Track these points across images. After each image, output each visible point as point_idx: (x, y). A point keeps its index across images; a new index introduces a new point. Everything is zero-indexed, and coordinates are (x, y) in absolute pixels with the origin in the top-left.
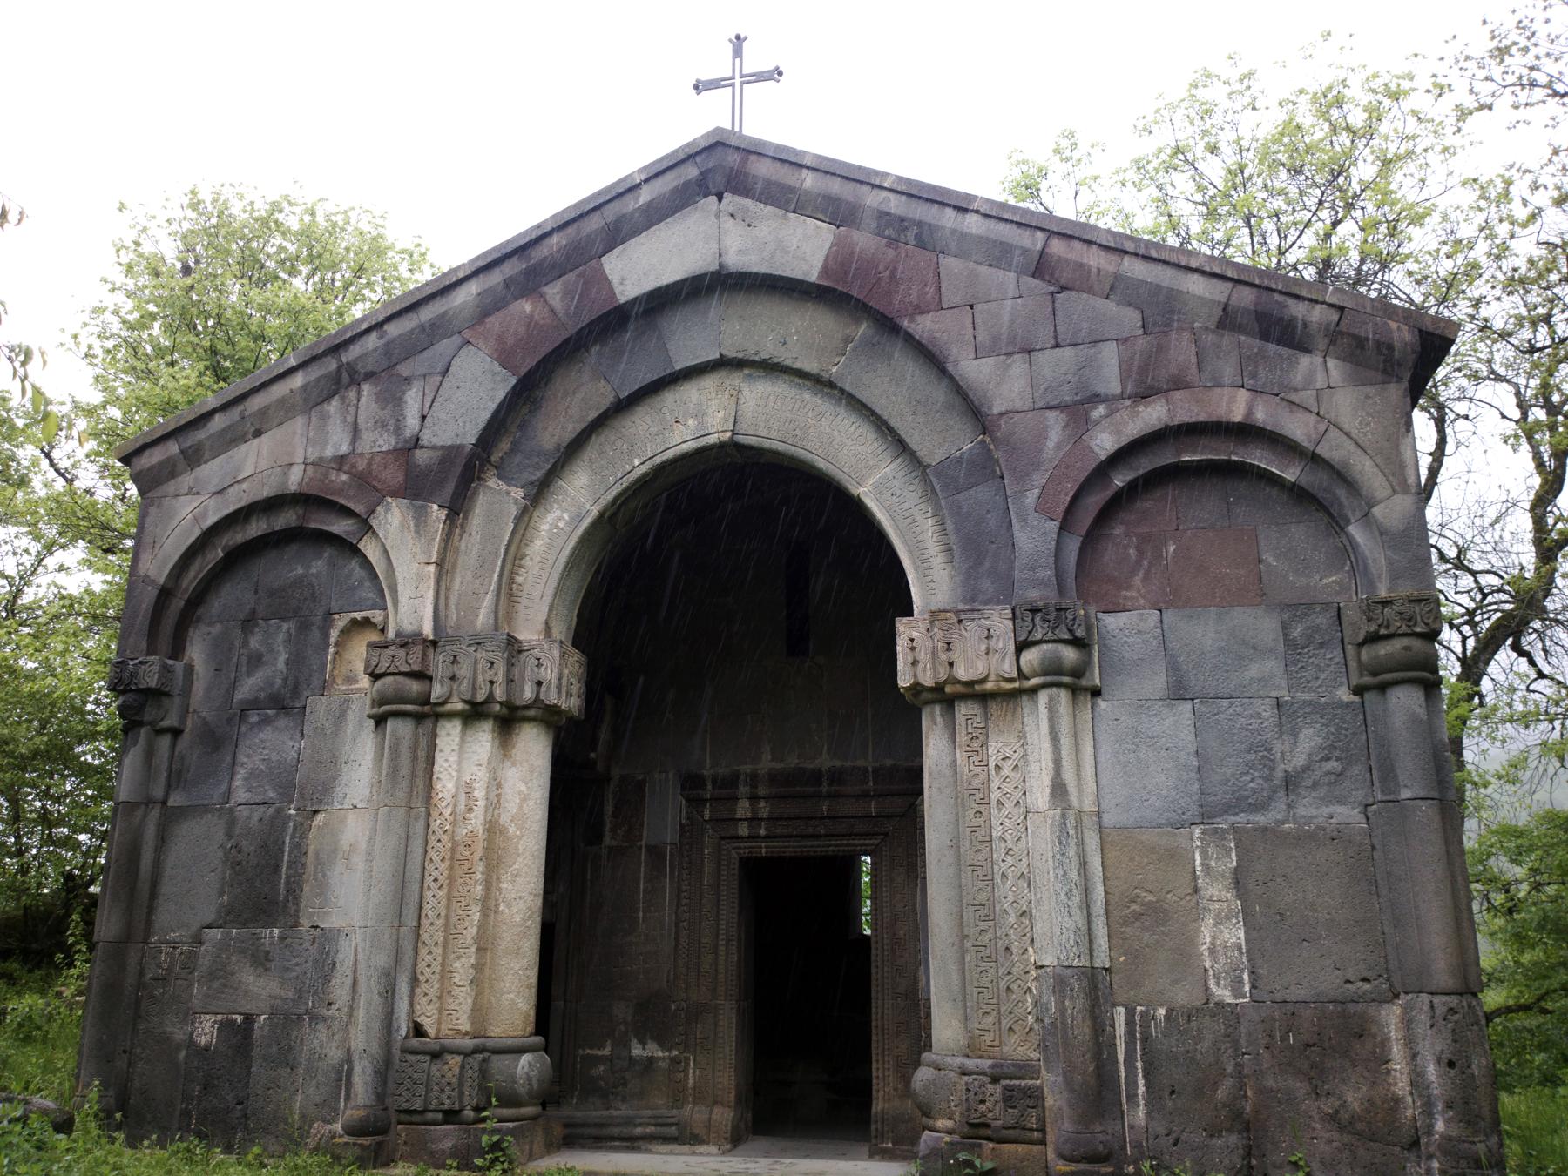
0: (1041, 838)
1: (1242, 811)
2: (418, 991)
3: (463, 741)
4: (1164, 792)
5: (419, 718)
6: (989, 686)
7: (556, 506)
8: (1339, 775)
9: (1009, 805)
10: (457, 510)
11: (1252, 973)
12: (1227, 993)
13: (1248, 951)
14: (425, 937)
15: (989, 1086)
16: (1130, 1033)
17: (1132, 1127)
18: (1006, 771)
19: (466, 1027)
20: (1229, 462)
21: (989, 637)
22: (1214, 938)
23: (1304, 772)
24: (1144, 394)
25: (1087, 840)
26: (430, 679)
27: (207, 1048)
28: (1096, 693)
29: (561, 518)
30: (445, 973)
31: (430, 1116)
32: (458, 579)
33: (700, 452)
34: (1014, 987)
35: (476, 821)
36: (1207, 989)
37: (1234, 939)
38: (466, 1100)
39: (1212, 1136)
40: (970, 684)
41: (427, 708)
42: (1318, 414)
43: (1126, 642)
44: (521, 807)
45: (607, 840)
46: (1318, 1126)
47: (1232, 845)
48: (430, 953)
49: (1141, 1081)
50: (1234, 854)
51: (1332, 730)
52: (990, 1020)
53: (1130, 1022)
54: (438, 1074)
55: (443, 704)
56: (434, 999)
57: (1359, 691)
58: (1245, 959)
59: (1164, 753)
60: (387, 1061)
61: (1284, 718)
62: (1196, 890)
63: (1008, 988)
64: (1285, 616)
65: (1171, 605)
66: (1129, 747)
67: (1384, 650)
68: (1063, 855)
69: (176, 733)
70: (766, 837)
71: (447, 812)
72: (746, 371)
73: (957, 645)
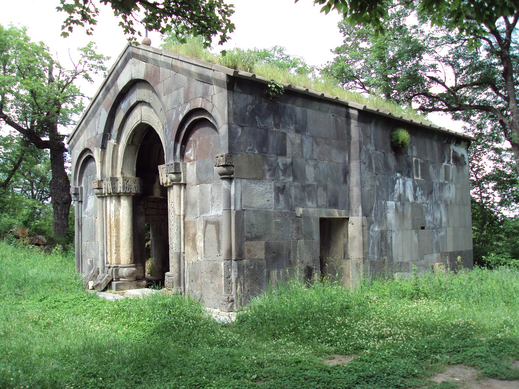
10: (104, 147)
24: (186, 102)
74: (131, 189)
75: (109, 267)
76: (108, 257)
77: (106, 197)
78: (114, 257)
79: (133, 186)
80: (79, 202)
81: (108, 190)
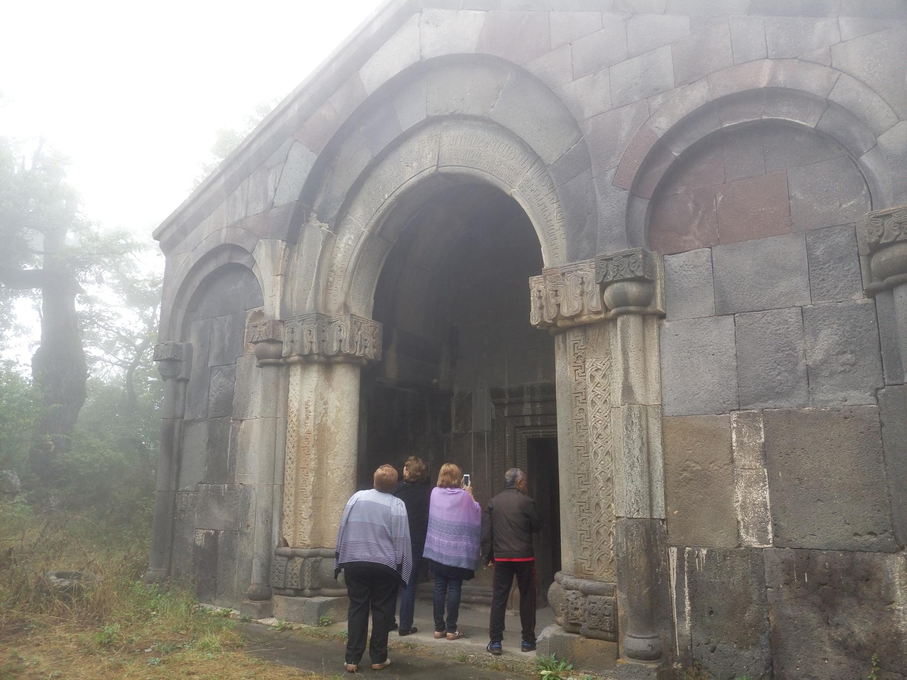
0: (617, 427)
1: (770, 399)
2: (284, 521)
3: (302, 378)
4: (710, 388)
5: (278, 365)
6: (584, 318)
7: (347, 231)
8: (853, 365)
9: (599, 404)
10: (293, 240)
11: (774, 525)
12: (755, 540)
13: (771, 508)
14: (286, 490)
15: (581, 598)
16: (680, 567)
17: (680, 635)
18: (598, 379)
19: (308, 542)
20: (764, 122)
21: (582, 283)
22: (745, 497)
23: (822, 364)
25: (651, 426)
26: (282, 342)
27: (200, 547)
28: (662, 316)
29: (350, 238)
30: (297, 511)
31: (288, 591)
32: (297, 282)
33: (421, 182)
34: (602, 531)
35: (310, 425)
36: (739, 536)
37: (761, 498)
38: (306, 583)
39: (741, 648)
40: (572, 318)
41: (281, 360)
42: (831, 67)
43: (685, 275)
44: (337, 415)
45: (454, 430)
46: (829, 650)
47: (761, 426)
48: (288, 500)
49: (687, 603)
50: (762, 433)
51: (847, 328)
52: (588, 553)
53: (680, 558)
54: (291, 569)
55: (289, 357)
56: (291, 526)
57: (871, 293)
58: (769, 514)
59: (711, 357)
60: (269, 560)
61: (806, 322)
62: (732, 461)
63: (598, 532)
64: (809, 240)
65: (719, 242)
66: (685, 354)
67: (884, 257)
68: (628, 437)
69: (186, 381)
70: (542, 426)
71: (294, 420)
72: (444, 124)
73: (562, 291)
74: (366, 347)
75: (291, 557)
76: (285, 526)
77: (289, 365)
78: (306, 527)
79: (370, 341)
80: (179, 381)
81: (302, 346)
